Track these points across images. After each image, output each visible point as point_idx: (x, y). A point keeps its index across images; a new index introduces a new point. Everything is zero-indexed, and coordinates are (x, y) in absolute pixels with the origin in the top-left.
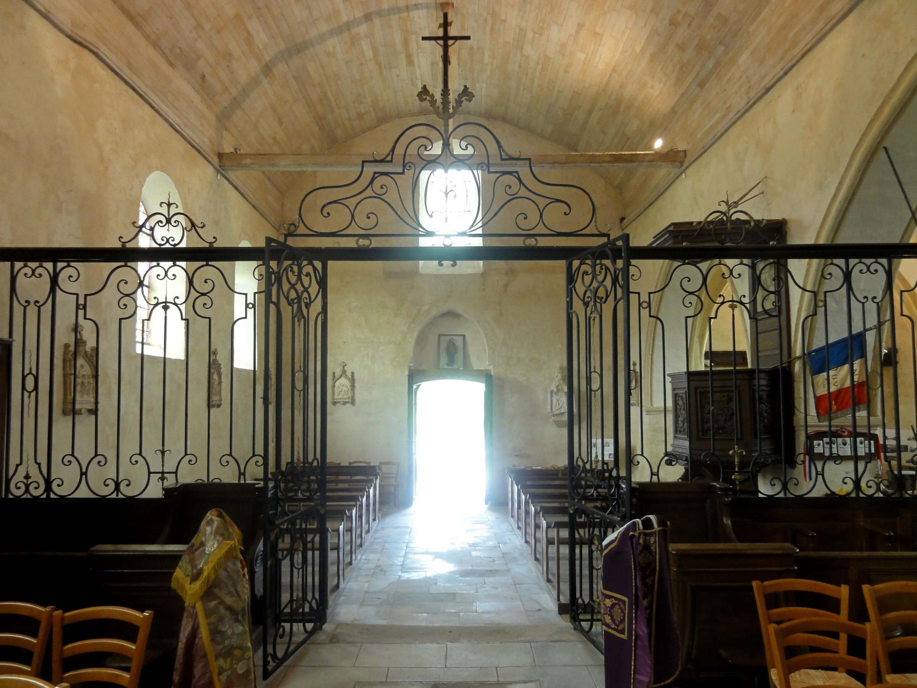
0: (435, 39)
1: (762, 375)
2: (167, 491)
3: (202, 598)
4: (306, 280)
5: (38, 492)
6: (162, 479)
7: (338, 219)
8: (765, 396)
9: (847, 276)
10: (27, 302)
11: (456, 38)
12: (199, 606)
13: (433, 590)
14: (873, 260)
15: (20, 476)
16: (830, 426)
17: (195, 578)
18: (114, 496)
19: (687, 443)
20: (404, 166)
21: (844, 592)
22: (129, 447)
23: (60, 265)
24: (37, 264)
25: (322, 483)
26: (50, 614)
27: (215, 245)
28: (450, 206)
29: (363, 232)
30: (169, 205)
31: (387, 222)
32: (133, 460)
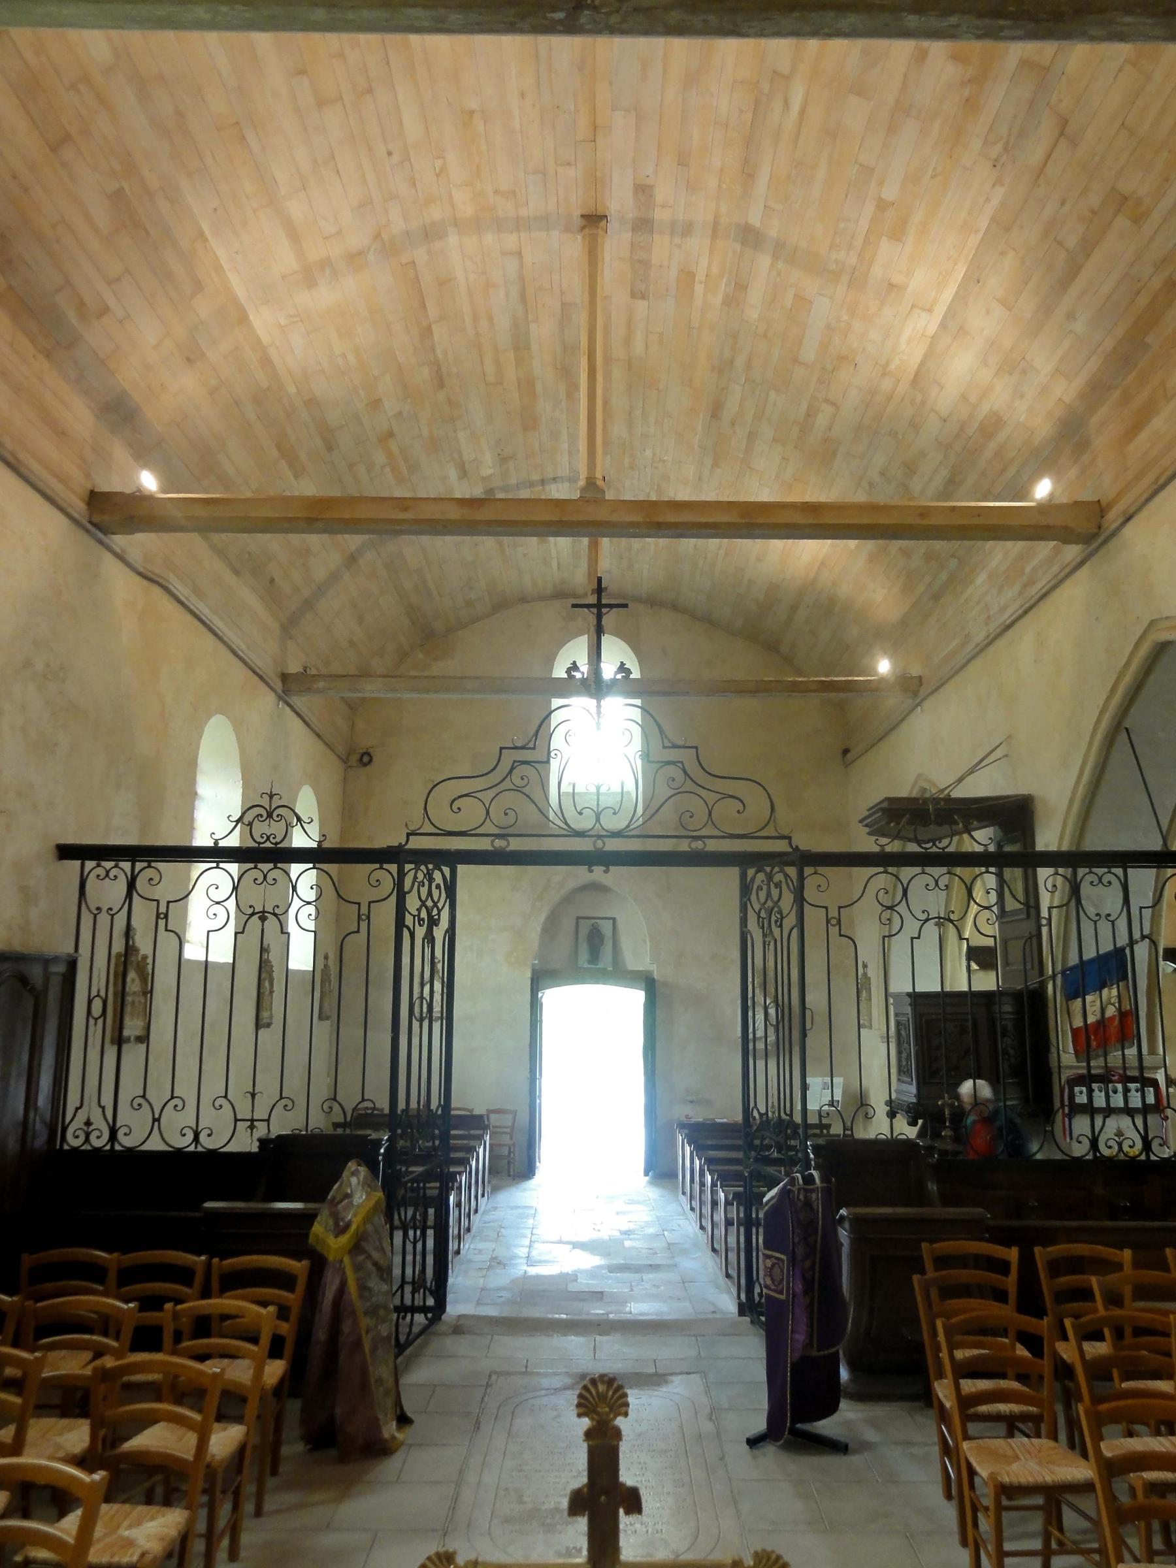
0: (588, 606)
1: (1005, 999)
2: (263, 1142)
3: (350, 1252)
4: (435, 893)
5: (99, 1141)
6: (252, 1127)
7: (470, 815)
8: (1010, 1025)
9: (1075, 890)
10: (98, 909)
11: (611, 606)
12: (347, 1260)
13: (572, 1287)
14: (1106, 870)
15: (79, 1122)
16: (1089, 1067)
17: (340, 1231)
18: (192, 1148)
19: (913, 1089)
21: (1013, 1254)
22: (213, 1086)
23: (139, 866)
24: (112, 864)
25: (445, 1137)
26: (209, 1264)
27: (326, 845)
28: (599, 751)
29: (497, 831)
30: (271, 796)
31: (528, 813)
32: (217, 1104)
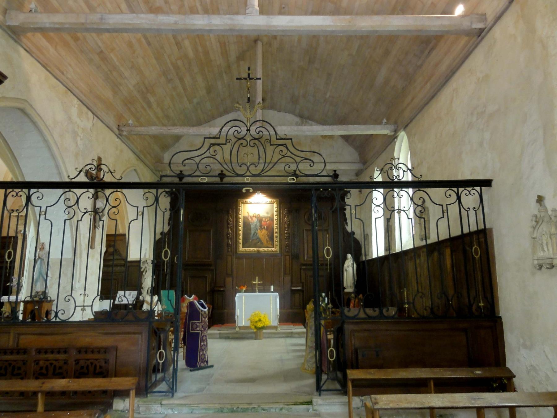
9: (459, 198)
18: (54, 320)
20: (226, 141)
32: (67, 299)
